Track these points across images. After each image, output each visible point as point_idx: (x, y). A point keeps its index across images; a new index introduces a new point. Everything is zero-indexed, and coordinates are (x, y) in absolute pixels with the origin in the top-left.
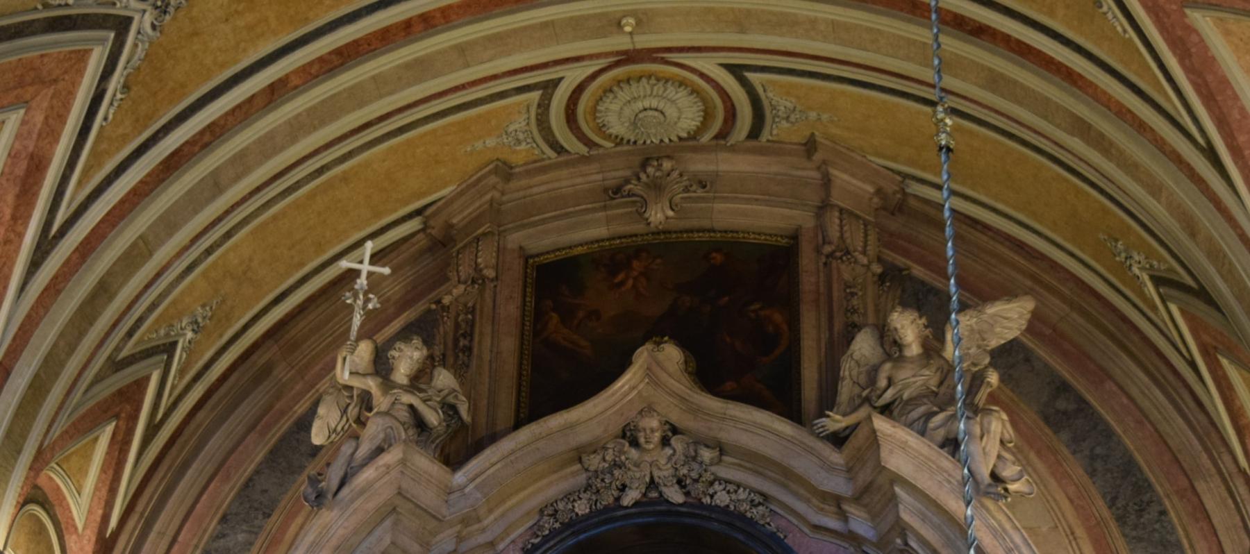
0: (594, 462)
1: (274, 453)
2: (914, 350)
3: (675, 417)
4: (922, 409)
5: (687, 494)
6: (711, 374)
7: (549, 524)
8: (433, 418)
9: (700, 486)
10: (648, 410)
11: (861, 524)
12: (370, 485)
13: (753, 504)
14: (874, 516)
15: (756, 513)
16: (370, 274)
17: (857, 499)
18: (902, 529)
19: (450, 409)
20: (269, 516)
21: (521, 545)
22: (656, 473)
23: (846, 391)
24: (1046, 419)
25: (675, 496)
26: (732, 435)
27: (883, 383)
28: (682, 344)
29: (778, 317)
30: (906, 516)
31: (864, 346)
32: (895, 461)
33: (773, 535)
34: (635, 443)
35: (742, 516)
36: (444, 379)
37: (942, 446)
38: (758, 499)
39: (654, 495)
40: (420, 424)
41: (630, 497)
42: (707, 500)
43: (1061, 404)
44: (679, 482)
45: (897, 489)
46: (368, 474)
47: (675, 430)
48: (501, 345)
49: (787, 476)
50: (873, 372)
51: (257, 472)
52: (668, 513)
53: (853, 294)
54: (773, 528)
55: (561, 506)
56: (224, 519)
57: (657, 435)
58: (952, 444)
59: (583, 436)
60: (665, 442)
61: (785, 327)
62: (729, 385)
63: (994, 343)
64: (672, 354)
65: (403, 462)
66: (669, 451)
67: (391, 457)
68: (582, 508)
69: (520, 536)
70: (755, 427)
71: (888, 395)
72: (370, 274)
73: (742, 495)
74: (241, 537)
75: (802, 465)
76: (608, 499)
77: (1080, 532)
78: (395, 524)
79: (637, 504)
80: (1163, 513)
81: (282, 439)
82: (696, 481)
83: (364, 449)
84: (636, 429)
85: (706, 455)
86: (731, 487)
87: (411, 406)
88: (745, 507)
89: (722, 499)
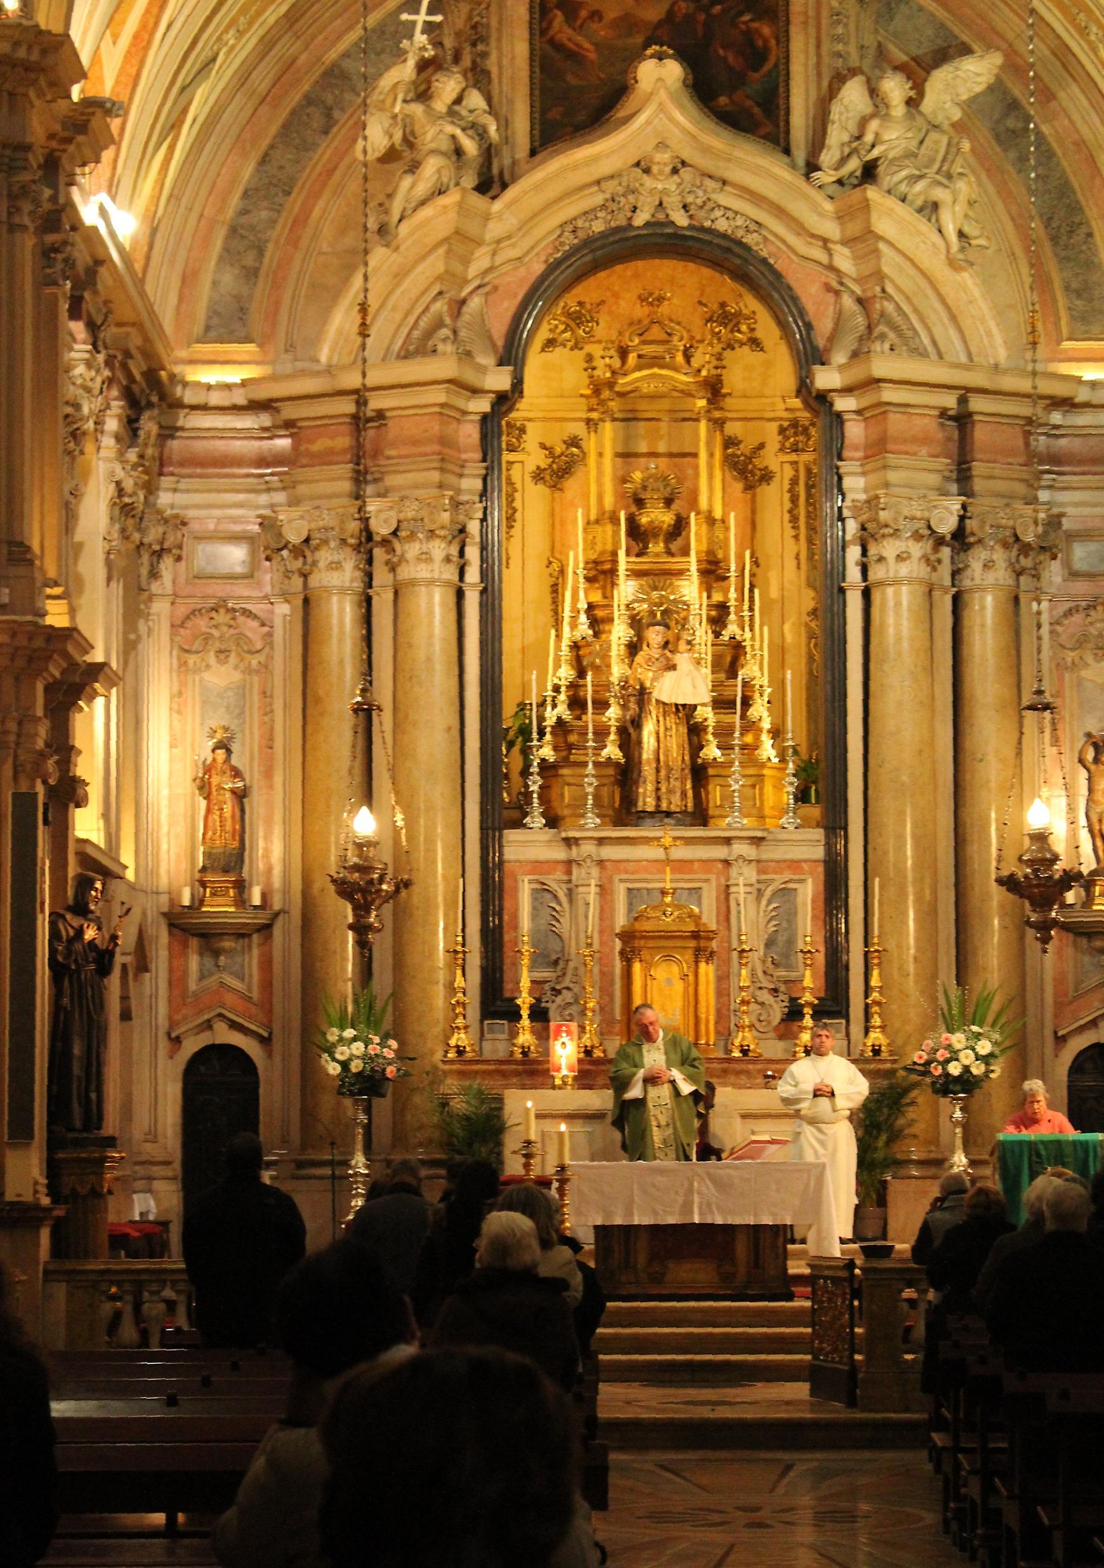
0: (611, 187)
1: (286, 126)
2: (898, 110)
3: (685, 155)
4: (904, 173)
5: (691, 217)
6: (704, 90)
7: (569, 240)
8: (470, 146)
9: (702, 214)
10: (662, 145)
11: (844, 260)
12: (428, 220)
13: (747, 230)
14: (856, 258)
15: (750, 239)
16: (417, 12)
17: (845, 242)
18: (879, 276)
19: (479, 132)
20: (289, 194)
21: (543, 258)
22: (665, 200)
23: (837, 137)
24: (997, 137)
25: (681, 219)
26: (735, 174)
27: (869, 138)
28: (682, 56)
29: (766, 30)
30: (886, 269)
31: (853, 95)
32: (882, 225)
33: (764, 261)
34: (647, 171)
35: (739, 243)
36: (476, 100)
37: (920, 210)
38: (753, 227)
39: (661, 216)
40: (459, 152)
41: (640, 219)
42: (707, 224)
43: (1011, 123)
44: (684, 207)
45: (881, 246)
46: (426, 212)
47: (683, 163)
48: (513, 54)
49: (780, 212)
50: (863, 122)
51: (272, 147)
52: (674, 236)
53: (839, 22)
54: (764, 254)
55: (580, 223)
56: (246, 194)
57: (668, 169)
58: (931, 209)
59: (605, 168)
60: (675, 171)
61: (773, 42)
62: (723, 100)
63: (964, 97)
64: (673, 71)
65: (460, 205)
66: (675, 177)
67: (452, 198)
68: (598, 227)
69: (544, 249)
70: (752, 165)
71: (875, 153)
72: (417, 12)
73: (740, 221)
74: (264, 214)
75: (799, 209)
76: (621, 221)
77: (1019, 252)
78: (448, 252)
79: (647, 224)
80: (1090, 235)
81: (293, 112)
82: (701, 207)
83: (423, 188)
84: (651, 161)
85: (710, 184)
86: (730, 214)
87: (453, 137)
88: (740, 233)
89: (722, 225)
